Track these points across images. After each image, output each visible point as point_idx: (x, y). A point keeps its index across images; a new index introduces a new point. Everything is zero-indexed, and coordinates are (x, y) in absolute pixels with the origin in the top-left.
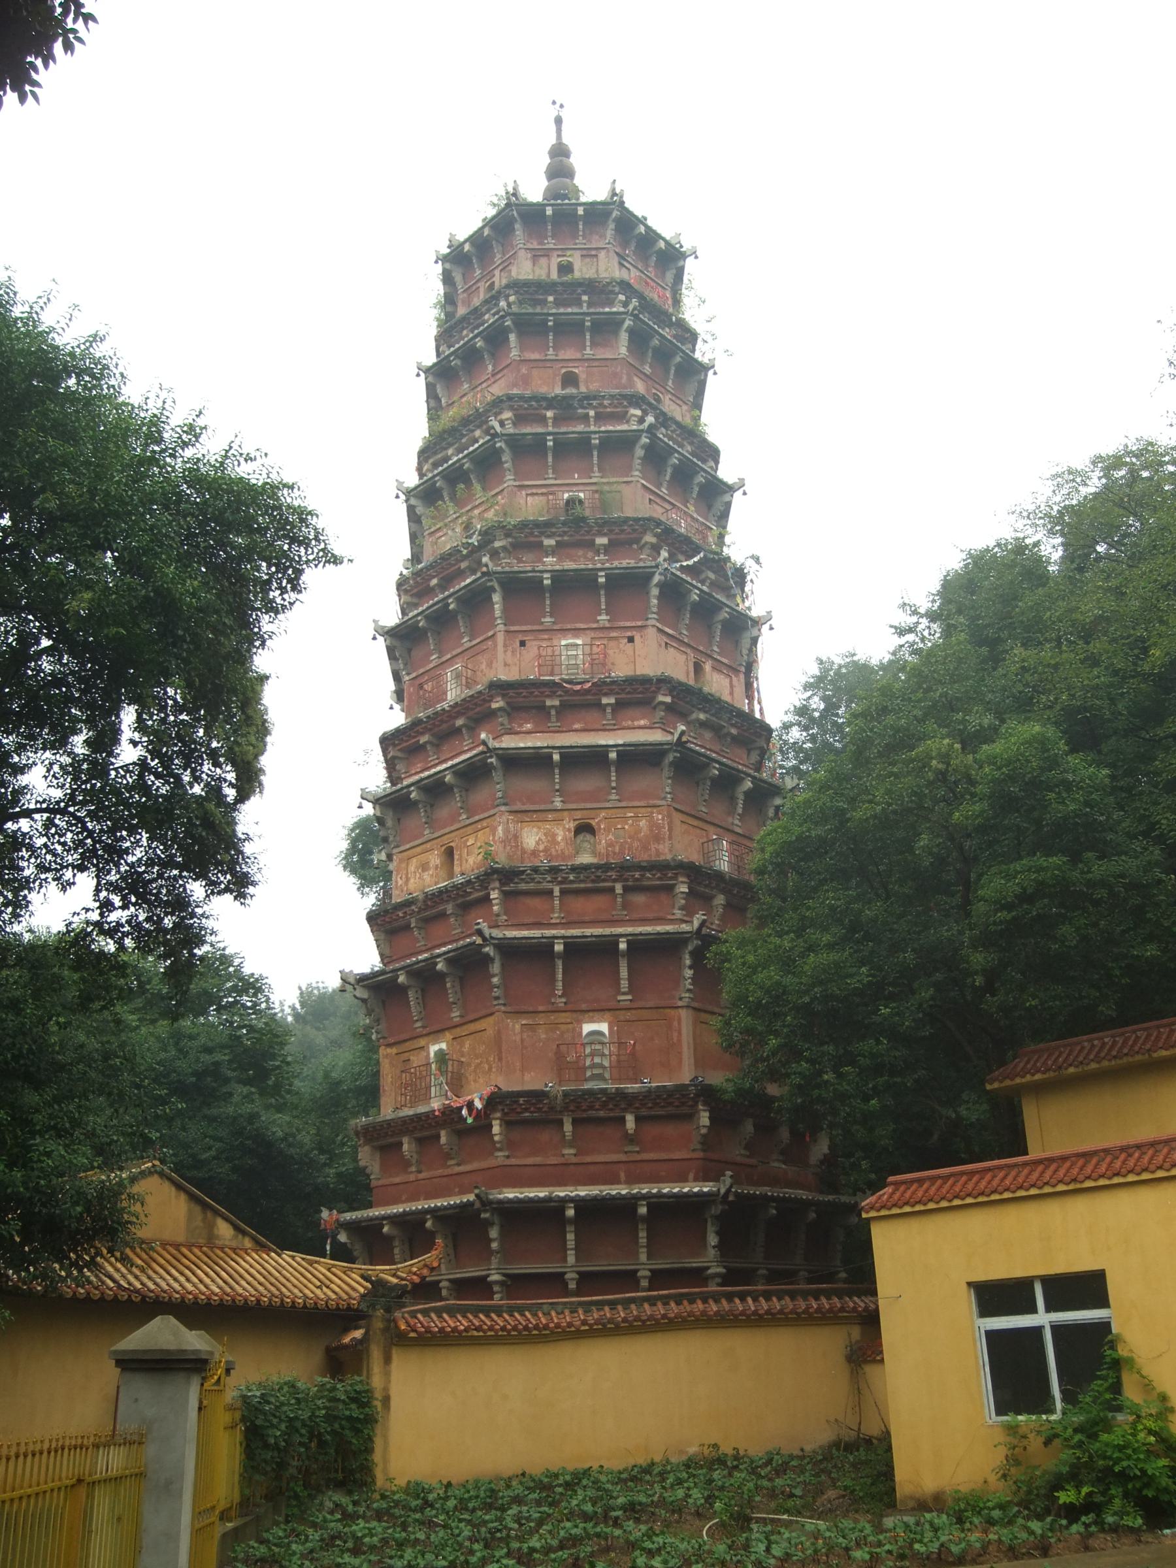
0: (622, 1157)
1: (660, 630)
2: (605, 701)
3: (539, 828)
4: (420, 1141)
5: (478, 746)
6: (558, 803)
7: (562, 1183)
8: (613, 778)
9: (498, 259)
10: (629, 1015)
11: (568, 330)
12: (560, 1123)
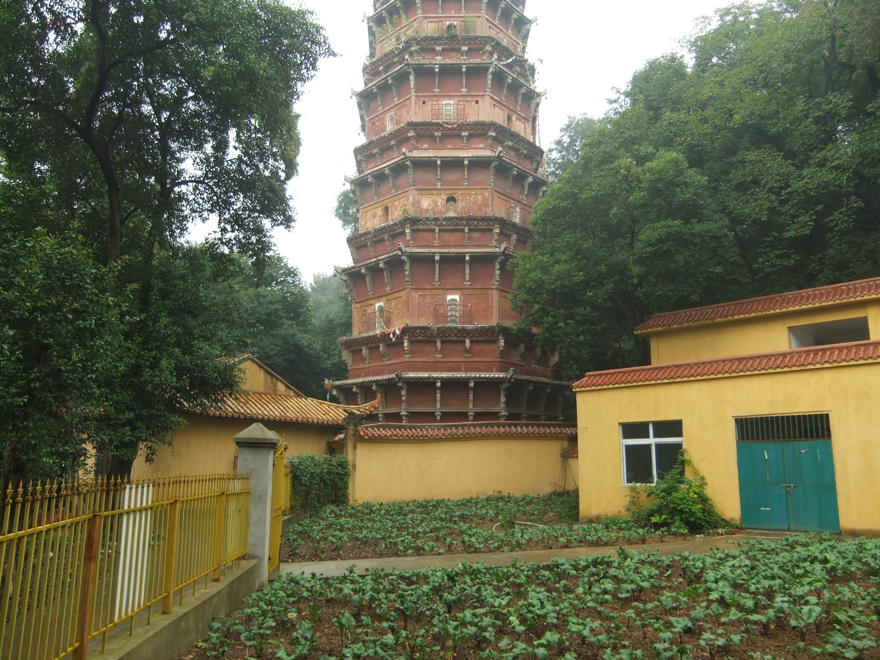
1: (492, 98)
4: (370, 349)
6: (439, 186)
7: (435, 371)
10: (469, 292)
12: (435, 342)
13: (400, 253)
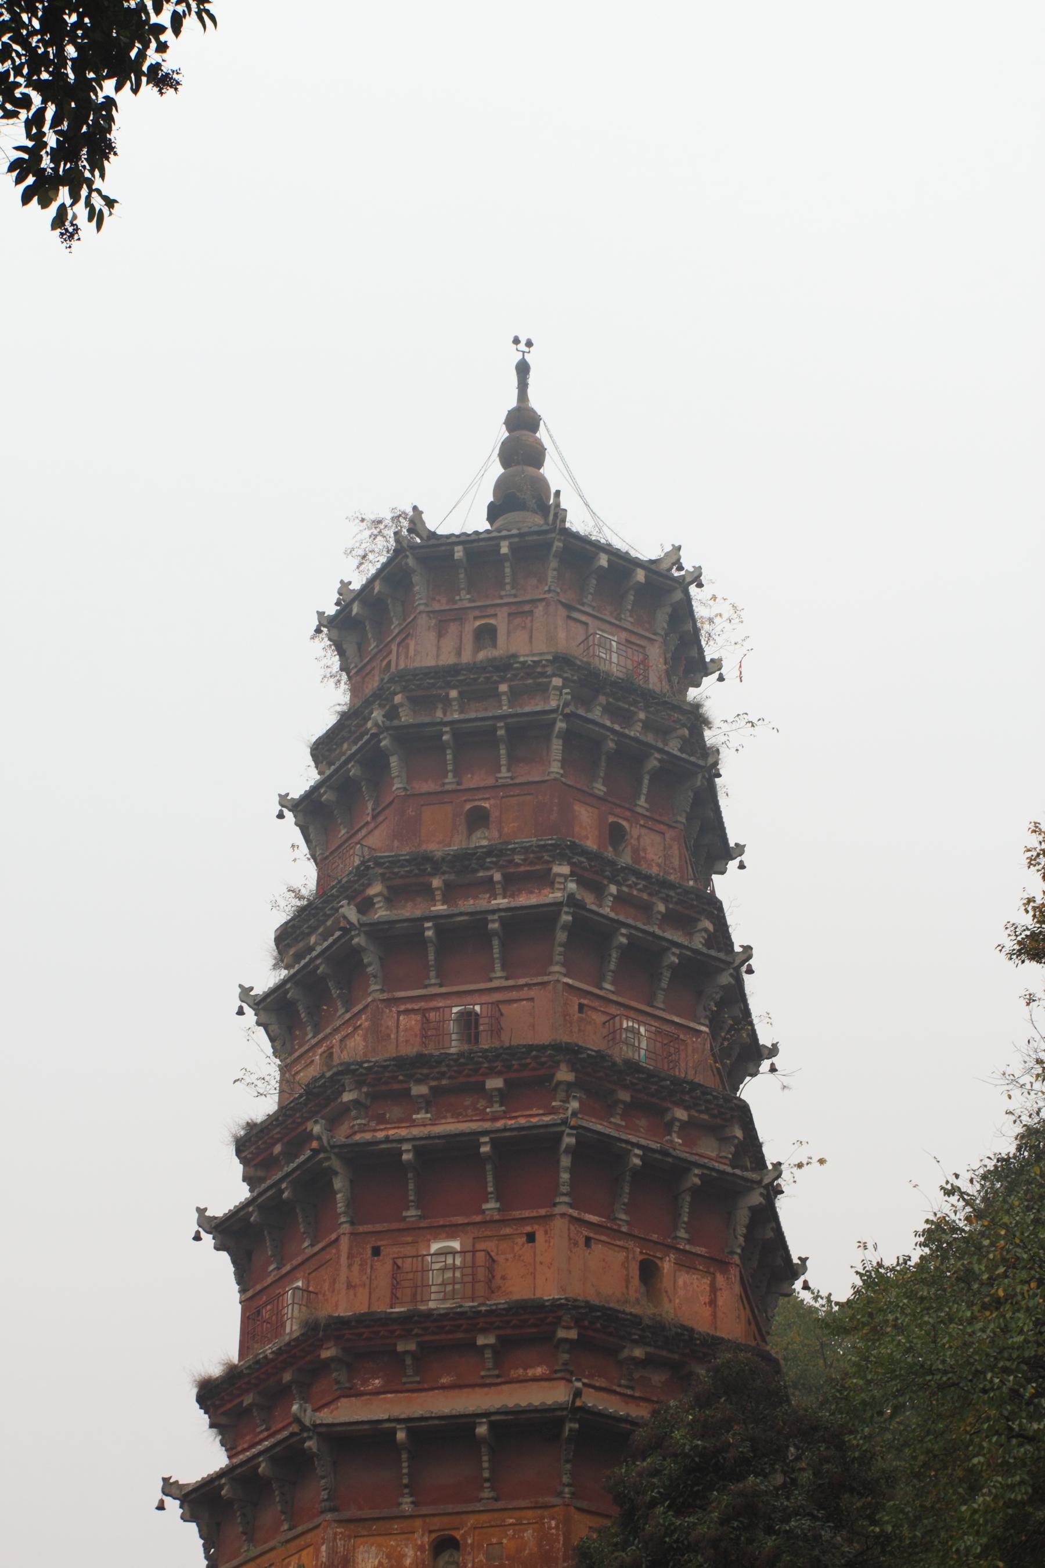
2: (481, 1341)
3: (380, 1546)
5: (290, 1424)
6: (406, 1505)
8: (486, 1465)
11: (474, 741)
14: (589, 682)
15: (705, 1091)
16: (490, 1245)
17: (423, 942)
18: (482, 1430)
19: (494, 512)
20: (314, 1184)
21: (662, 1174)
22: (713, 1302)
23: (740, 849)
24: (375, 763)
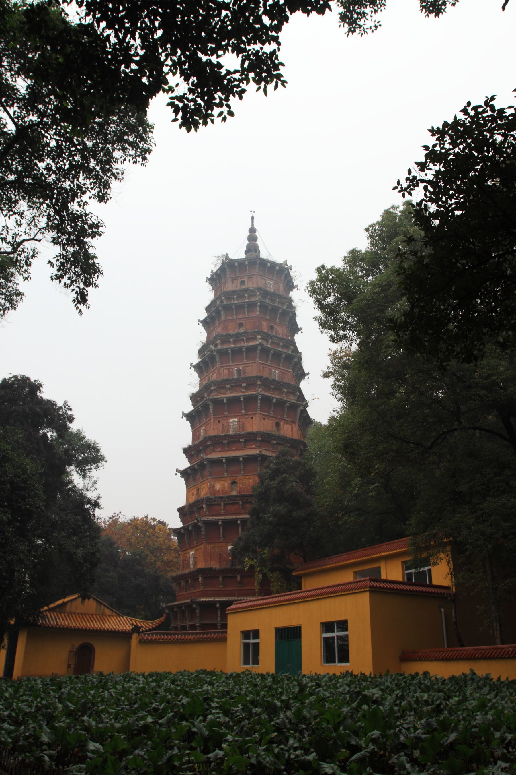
0: (237, 588)
6: (226, 475)
7: (218, 596)
9: (223, 281)
13: (196, 521)
14: (265, 293)
15: (291, 385)
16: (243, 420)
17: (229, 354)
18: (241, 459)
19: (246, 252)
20: (206, 407)
21: (281, 403)
22: (292, 431)
23: (301, 329)
24: (218, 312)
